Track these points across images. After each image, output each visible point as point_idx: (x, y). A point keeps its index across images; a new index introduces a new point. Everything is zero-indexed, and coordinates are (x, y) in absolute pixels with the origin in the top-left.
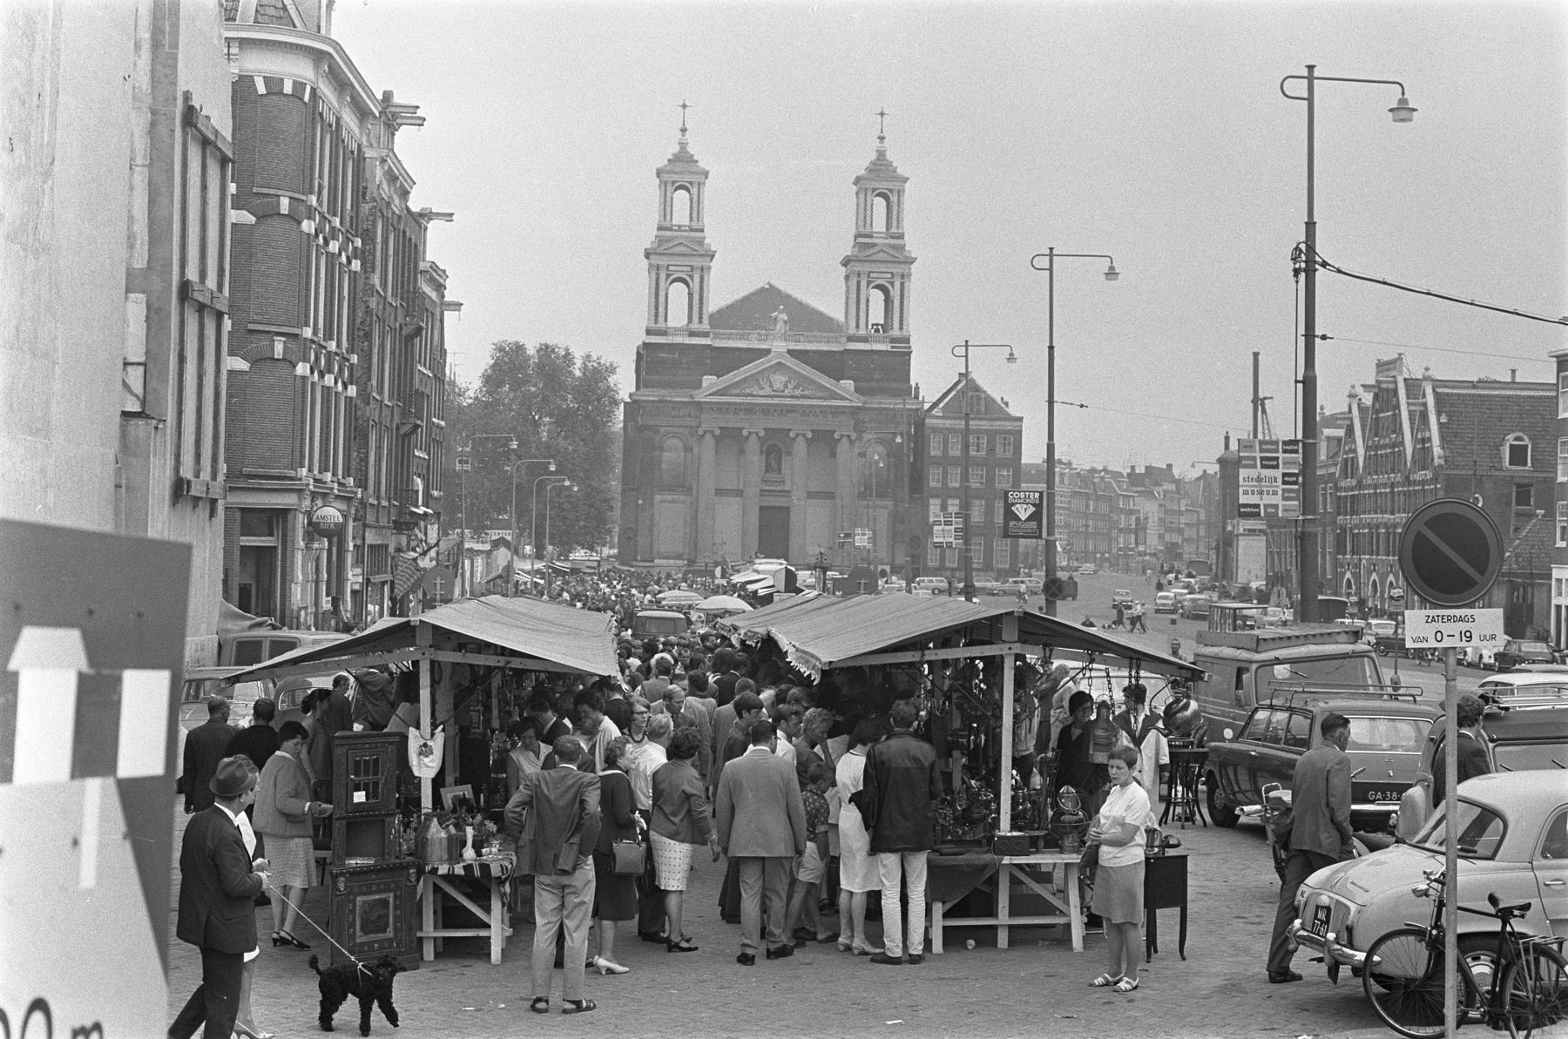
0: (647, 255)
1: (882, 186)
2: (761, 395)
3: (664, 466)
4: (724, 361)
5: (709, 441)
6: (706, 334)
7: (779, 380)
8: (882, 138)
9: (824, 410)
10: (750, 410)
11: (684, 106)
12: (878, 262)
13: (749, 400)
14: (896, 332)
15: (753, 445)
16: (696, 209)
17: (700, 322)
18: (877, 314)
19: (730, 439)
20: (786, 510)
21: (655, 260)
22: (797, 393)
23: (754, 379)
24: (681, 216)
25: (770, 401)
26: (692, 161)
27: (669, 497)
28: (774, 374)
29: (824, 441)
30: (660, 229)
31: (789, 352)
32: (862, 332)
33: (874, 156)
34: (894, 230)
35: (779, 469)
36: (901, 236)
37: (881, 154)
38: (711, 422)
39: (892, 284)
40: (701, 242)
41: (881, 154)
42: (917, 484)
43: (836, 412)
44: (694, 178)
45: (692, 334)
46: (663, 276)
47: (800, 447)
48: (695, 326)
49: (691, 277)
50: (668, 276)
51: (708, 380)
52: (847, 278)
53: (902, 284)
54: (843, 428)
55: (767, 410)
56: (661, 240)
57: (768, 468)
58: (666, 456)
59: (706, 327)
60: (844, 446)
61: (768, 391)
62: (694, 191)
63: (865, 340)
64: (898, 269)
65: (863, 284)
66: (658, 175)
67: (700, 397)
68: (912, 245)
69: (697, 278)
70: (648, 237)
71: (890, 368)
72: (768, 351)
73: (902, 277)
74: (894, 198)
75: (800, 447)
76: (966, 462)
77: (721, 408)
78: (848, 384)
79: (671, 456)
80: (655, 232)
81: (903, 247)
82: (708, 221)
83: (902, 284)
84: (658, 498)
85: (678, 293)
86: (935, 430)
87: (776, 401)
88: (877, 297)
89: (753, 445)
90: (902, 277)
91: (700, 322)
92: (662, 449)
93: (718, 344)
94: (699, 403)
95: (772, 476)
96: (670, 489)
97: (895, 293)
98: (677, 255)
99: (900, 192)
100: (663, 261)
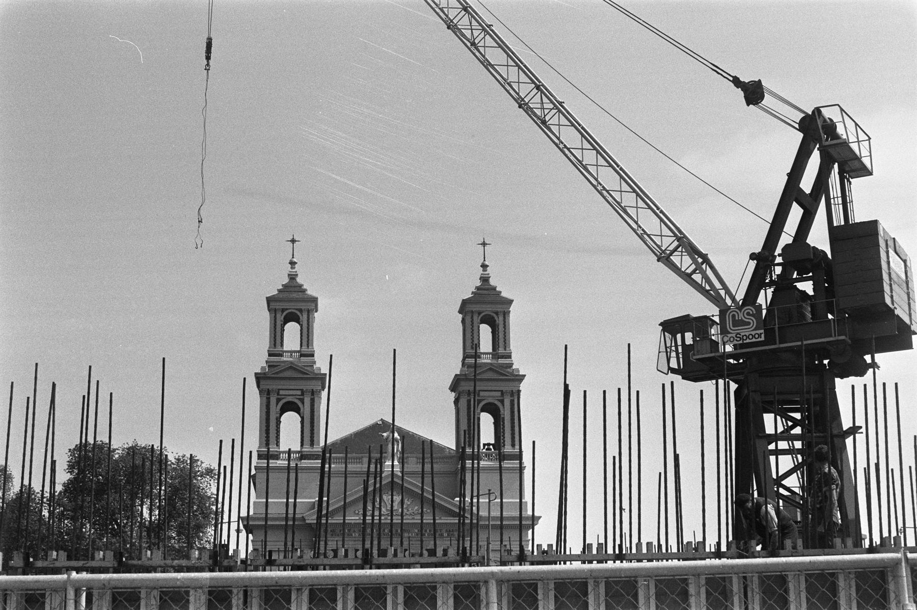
1: (488, 309)
8: (484, 266)
16: (306, 336)
17: (312, 444)
18: (487, 434)
26: (300, 289)
34: (501, 351)
36: (510, 357)
37: (485, 280)
39: (502, 402)
41: (485, 280)
44: (302, 306)
46: (273, 400)
48: (307, 449)
49: (302, 401)
50: (278, 400)
52: (456, 402)
56: (271, 365)
62: (304, 318)
64: (507, 387)
68: (519, 363)
69: (307, 400)
70: (259, 361)
74: (500, 320)
85: (290, 423)
90: (512, 394)
97: (506, 413)
98: (289, 385)
99: (506, 314)
100: (273, 385)
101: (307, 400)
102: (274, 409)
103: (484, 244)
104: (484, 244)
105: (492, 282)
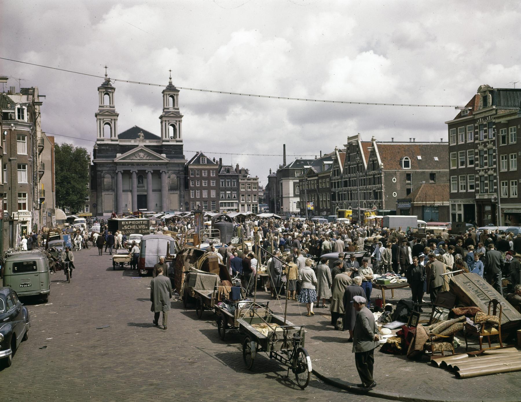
0: (96, 115)
1: (172, 93)
2: (136, 160)
3: (105, 183)
4: (124, 149)
5: (120, 175)
6: (117, 141)
7: (142, 154)
8: (170, 78)
9: (156, 164)
10: (132, 164)
11: (106, 67)
12: (171, 118)
13: (133, 161)
14: (178, 139)
15: (135, 176)
16: (111, 100)
17: (115, 136)
18: (171, 134)
19: (127, 174)
20: (146, 196)
21: (99, 117)
22: (148, 158)
23: (133, 154)
24: (107, 102)
25: (139, 161)
27: (107, 193)
28: (139, 153)
29: (157, 174)
30: (100, 107)
31: (146, 146)
32: (167, 139)
33: (168, 84)
34: (176, 107)
35: (143, 183)
36: (178, 109)
37: (170, 83)
38: (120, 169)
40: (114, 111)
41: (170, 83)
42: (187, 186)
43: (161, 164)
45: (112, 140)
47: (150, 175)
48: (113, 138)
49: (111, 122)
50: (103, 122)
51: (118, 155)
53: (179, 124)
54: (162, 169)
55: (138, 164)
56: (101, 111)
57: (139, 182)
58: (105, 180)
59: (117, 138)
60: (164, 174)
61: (138, 158)
62: (111, 95)
63: (168, 141)
65: (167, 124)
66: (98, 90)
67: (116, 160)
69: (113, 122)
71: (177, 151)
72: (137, 146)
73: (179, 121)
74: (175, 97)
75: (150, 175)
76: (202, 178)
77: (123, 164)
78: (164, 155)
79: (107, 180)
80: (98, 108)
81: (179, 112)
82: (115, 104)
83: (179, 124)
84: (103, 193)
86: (191, 169)
87: (141, 161)
88: (171, 128)
89: (135, 176)
91: (115, 136)
92: (104, 177)
93: (121, 144)
94: (116, 164)
95: (141, 185)
96: (108, 190)
97: (177, 127)
99: (177, 95)
101: (113, 122)
102: (102, 124)
103: (170, 71)
104: (170, 71)
105: (173, 84)
